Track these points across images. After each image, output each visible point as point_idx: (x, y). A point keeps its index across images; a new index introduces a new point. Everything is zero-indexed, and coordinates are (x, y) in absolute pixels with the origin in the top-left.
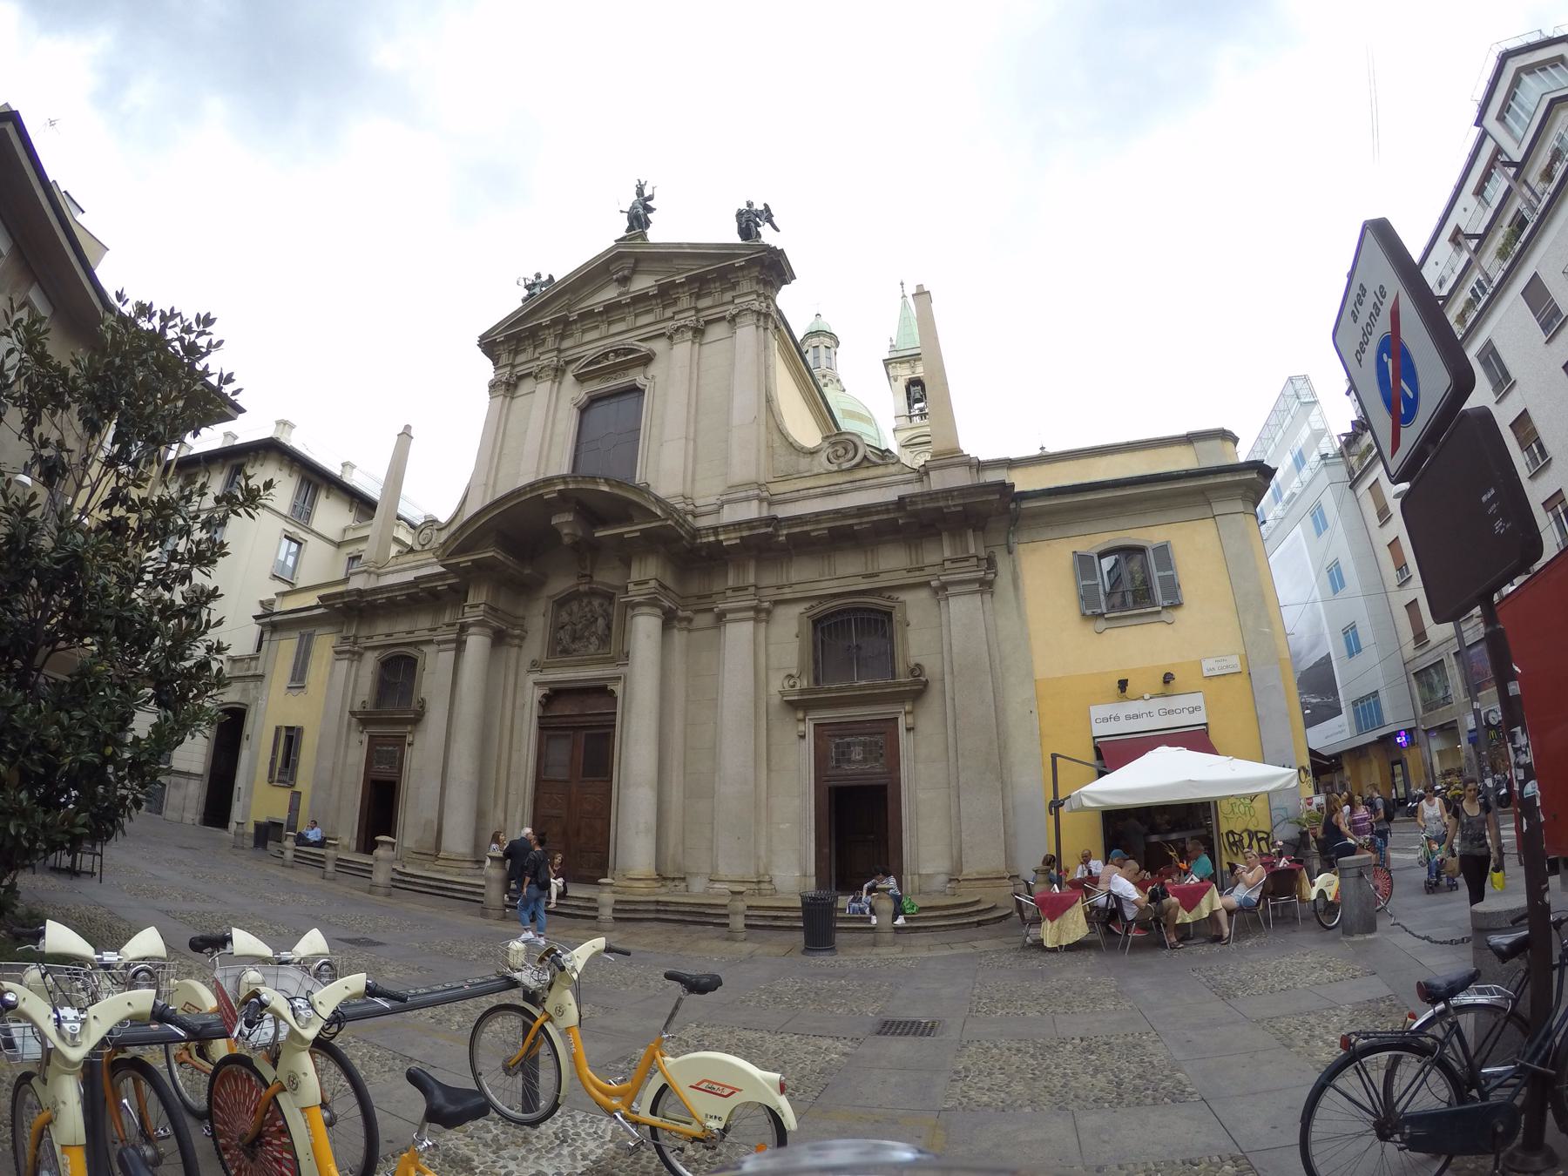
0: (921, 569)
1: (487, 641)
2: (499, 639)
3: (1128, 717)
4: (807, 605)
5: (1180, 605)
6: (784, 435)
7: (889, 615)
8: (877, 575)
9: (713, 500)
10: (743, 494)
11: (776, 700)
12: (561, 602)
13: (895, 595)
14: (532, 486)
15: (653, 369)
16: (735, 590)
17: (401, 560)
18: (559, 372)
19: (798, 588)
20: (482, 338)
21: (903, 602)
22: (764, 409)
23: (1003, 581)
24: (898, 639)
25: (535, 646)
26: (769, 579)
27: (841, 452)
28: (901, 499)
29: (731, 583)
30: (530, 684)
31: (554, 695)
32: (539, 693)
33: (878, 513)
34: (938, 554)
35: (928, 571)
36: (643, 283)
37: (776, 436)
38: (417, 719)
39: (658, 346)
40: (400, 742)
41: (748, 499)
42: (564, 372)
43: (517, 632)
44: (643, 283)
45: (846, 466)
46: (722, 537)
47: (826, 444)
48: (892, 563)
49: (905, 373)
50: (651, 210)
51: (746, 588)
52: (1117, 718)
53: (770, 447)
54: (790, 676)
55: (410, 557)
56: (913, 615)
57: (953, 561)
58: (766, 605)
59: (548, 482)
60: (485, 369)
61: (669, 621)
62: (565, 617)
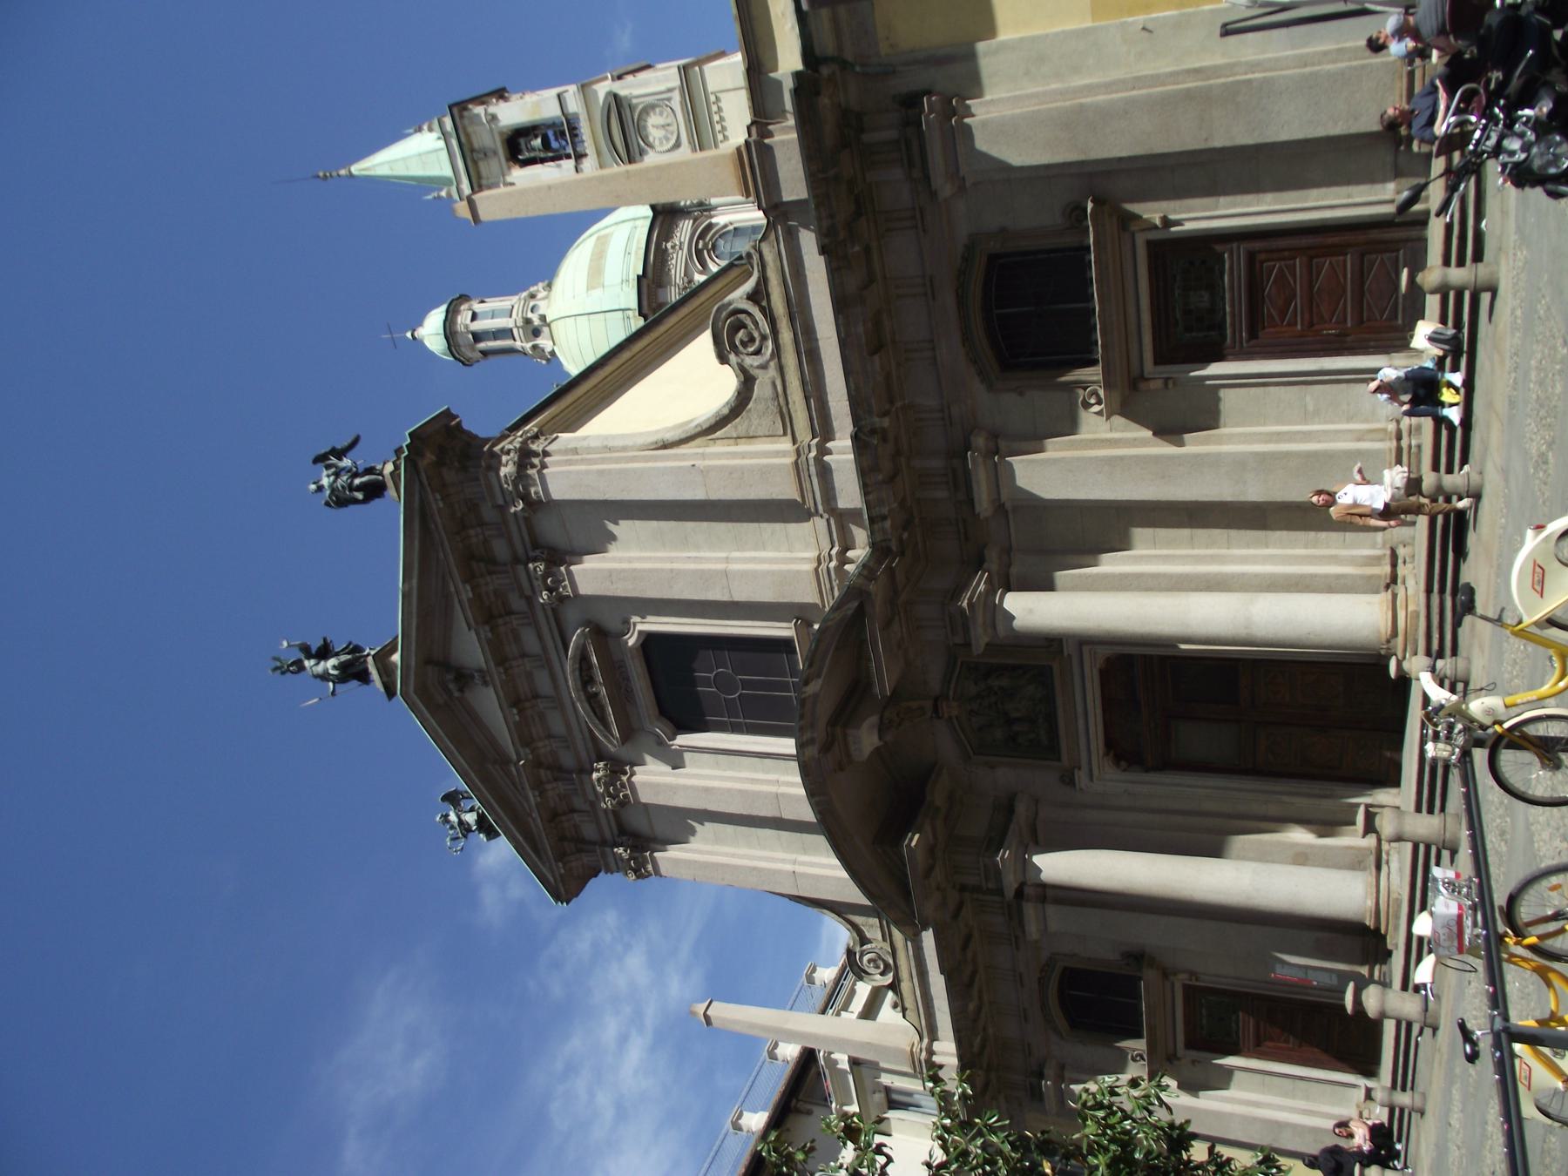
6: (721, 422)
7: (993, 258)
20: (558, 897)
28: (823, 250)
36: (470, 648)
44: (470, 648)
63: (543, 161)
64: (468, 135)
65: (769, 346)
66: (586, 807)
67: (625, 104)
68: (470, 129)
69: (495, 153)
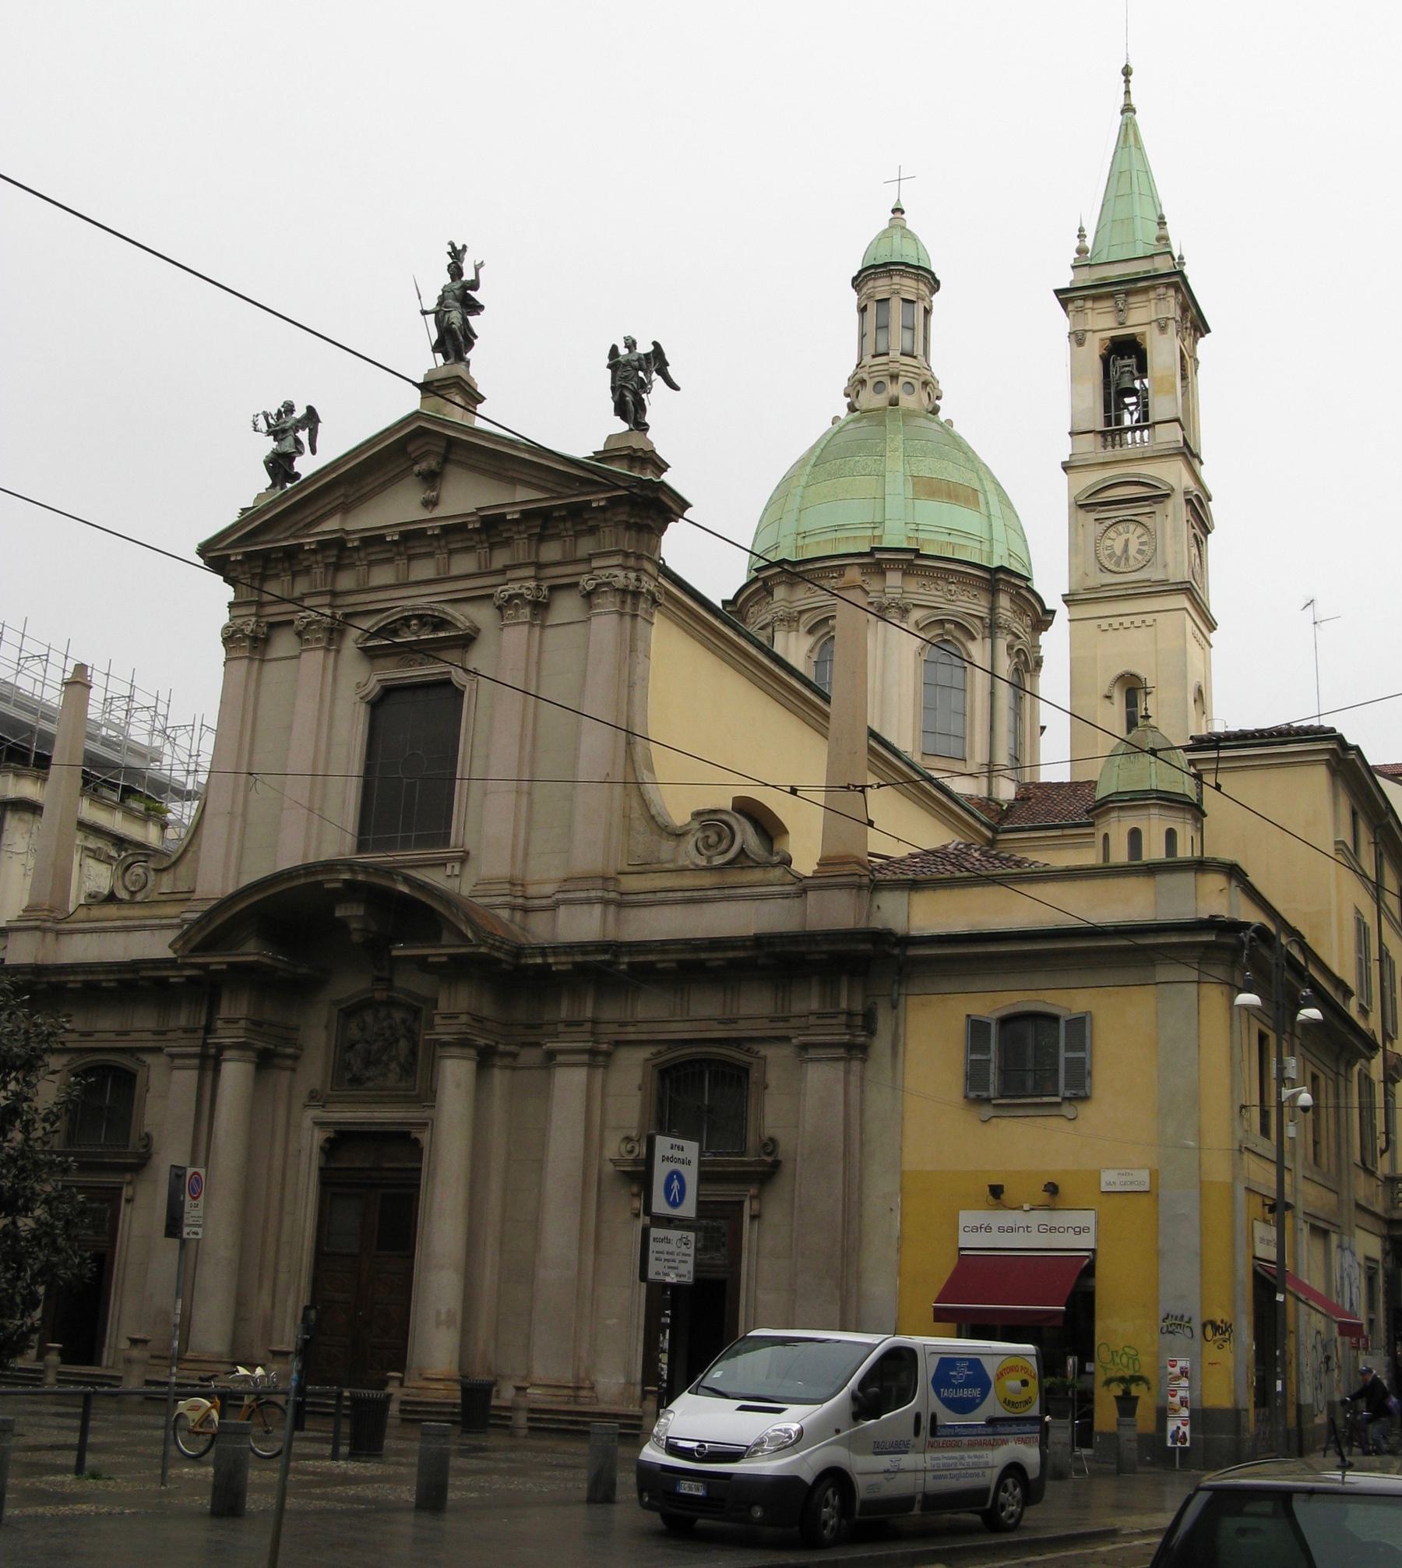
0: (786, 1019)
1: (249, 1068)
2: (264, 1062)
3: (1001, 1229)
4: (653, 1049)
5: (1086, 1098)
7: (747, 1071)
8: (734, 1021)
9: (549, 889)
10: (583, 895)
11: (609, 1168)
12: (350, 1012)
13: (756, 1047)
14: (308, 869)
15: (477, 658)
16: (569, 1024)
17: (96, 912)
18: (335, 632)
19: (644, 1027)
21: (765, 1058)
22: (621, 761)
23: (881, 1043)
24: (752, 1101)
25: (314, 1069)
26: (612, 1011)
27: (713, 839)
29: (563, 1014)
30: (307, 1123)
31: (340, 1141)
32: (319, 1137)
33: (734, 948)
34: (808, 1001)
35: (794, 1022)
37: (635, 803)
38: (140, 1163)
39: (482, 615)
40: (112, 1197)
41: (588, 902)
42: (342, 633)
43: (290, 1051)
45: (718, 860)
46: (551, 960)
47: (696, 825)
48: (755, 1006)
49: (1103, 322)
50: (475, 308)
51: (580, 1024)
52: (988, 1229)
53: (626, 816)
54: (628, 1139)
55: (112, 910)
56: (773, 1076)
57: (820, 1016)
58: (604, 1047)
59: (330, 866)
60: (214, 597)
61: (485, 1059)
62: (354, 1032)
63: (1107, 384)
64: (1145, 290)
65: (703, 862)
66: (297, 594)
67: (1155, 508)
68: (1152, 295)
69: (1122, 324)
